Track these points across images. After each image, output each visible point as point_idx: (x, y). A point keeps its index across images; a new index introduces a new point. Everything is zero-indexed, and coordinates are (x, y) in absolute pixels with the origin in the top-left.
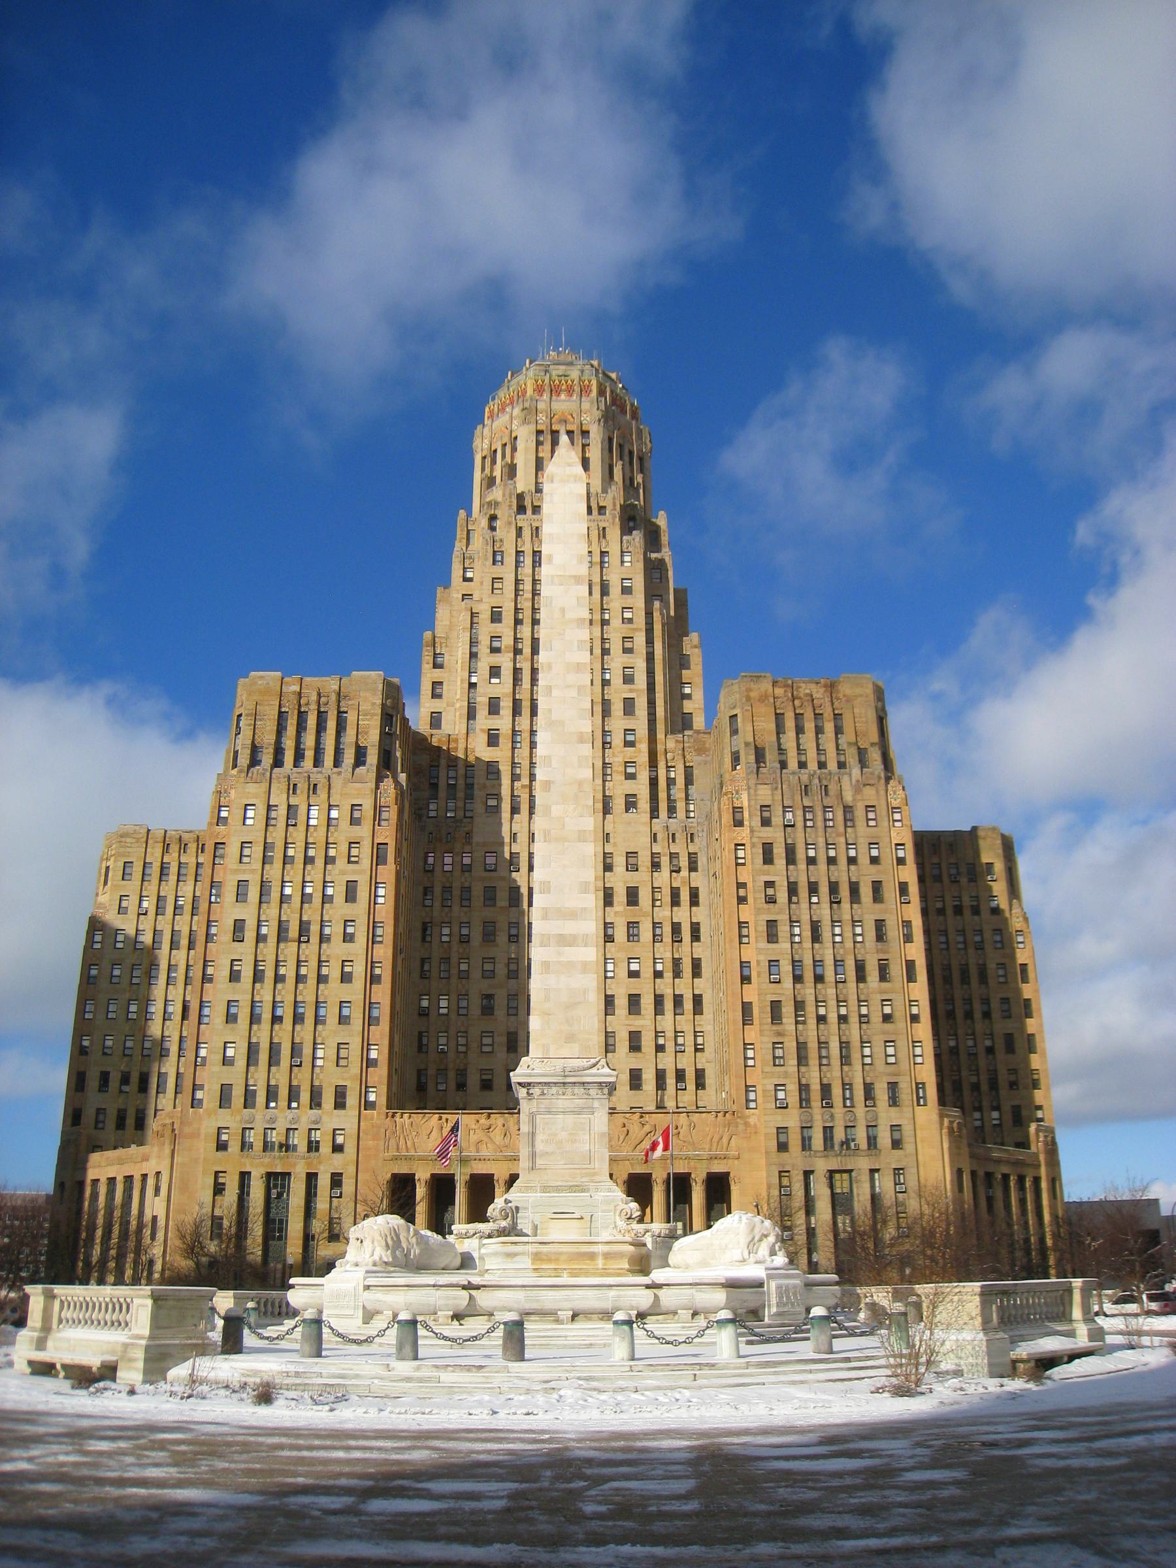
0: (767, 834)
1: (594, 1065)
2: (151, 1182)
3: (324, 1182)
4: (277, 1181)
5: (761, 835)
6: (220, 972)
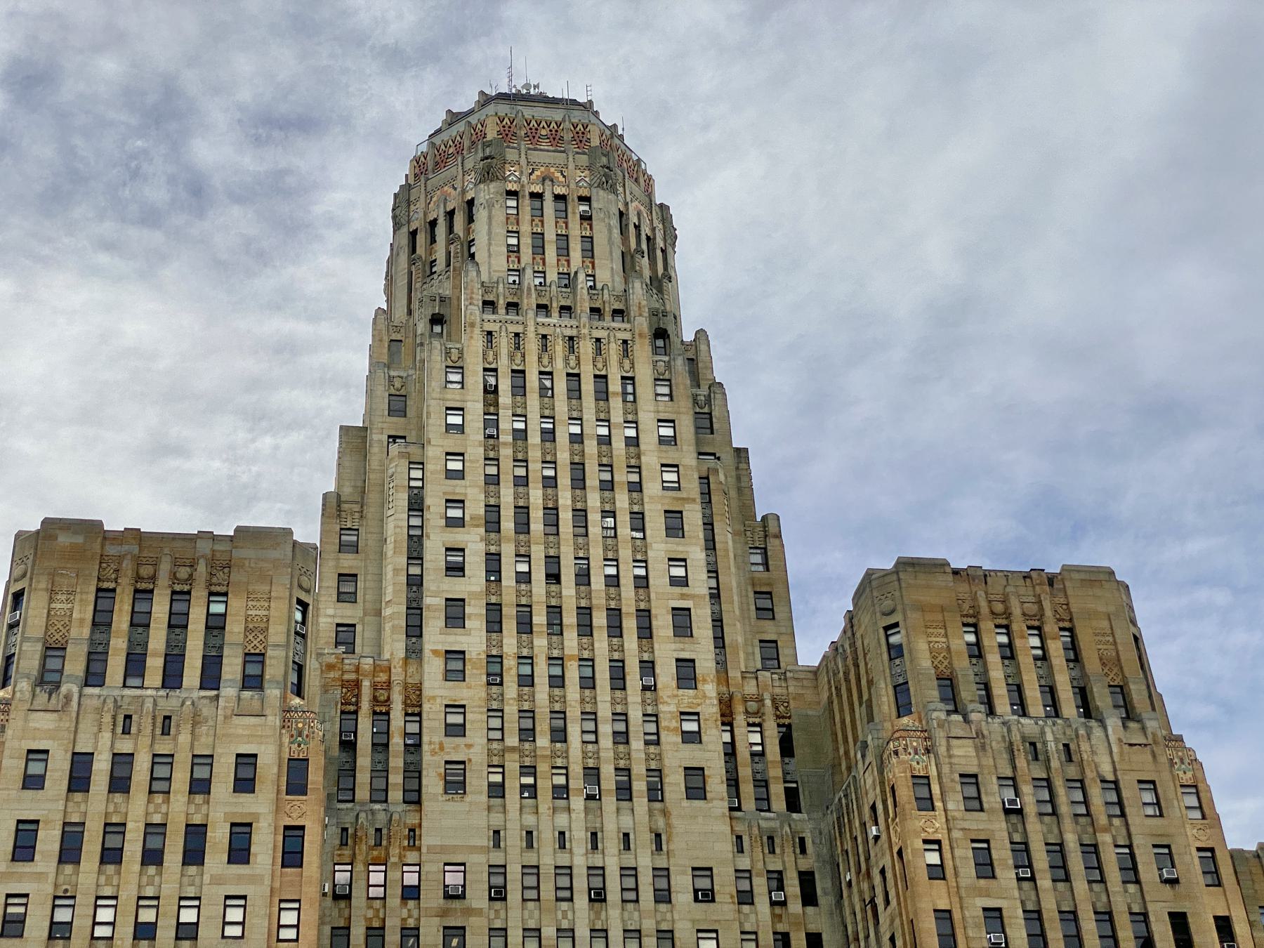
0: (978, 823)
5: (966, 825)
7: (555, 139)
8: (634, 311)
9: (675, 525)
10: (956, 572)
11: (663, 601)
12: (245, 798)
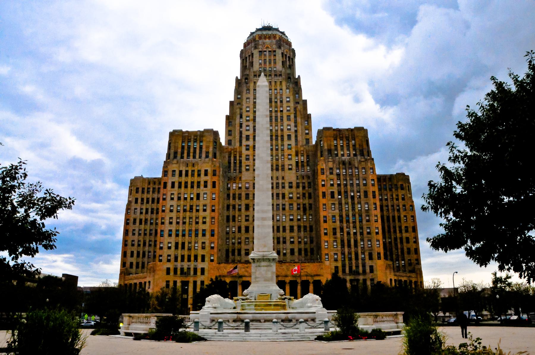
1: (271, 254)
2: (147, 284)
3: (199, 283)
4: (185, 284)
6: (167, 221)
7: (269, 38)
8: (283, 75)
9: (289, 118)
10: (334, 130)
11: (286, 133)
12: (206, 177)
